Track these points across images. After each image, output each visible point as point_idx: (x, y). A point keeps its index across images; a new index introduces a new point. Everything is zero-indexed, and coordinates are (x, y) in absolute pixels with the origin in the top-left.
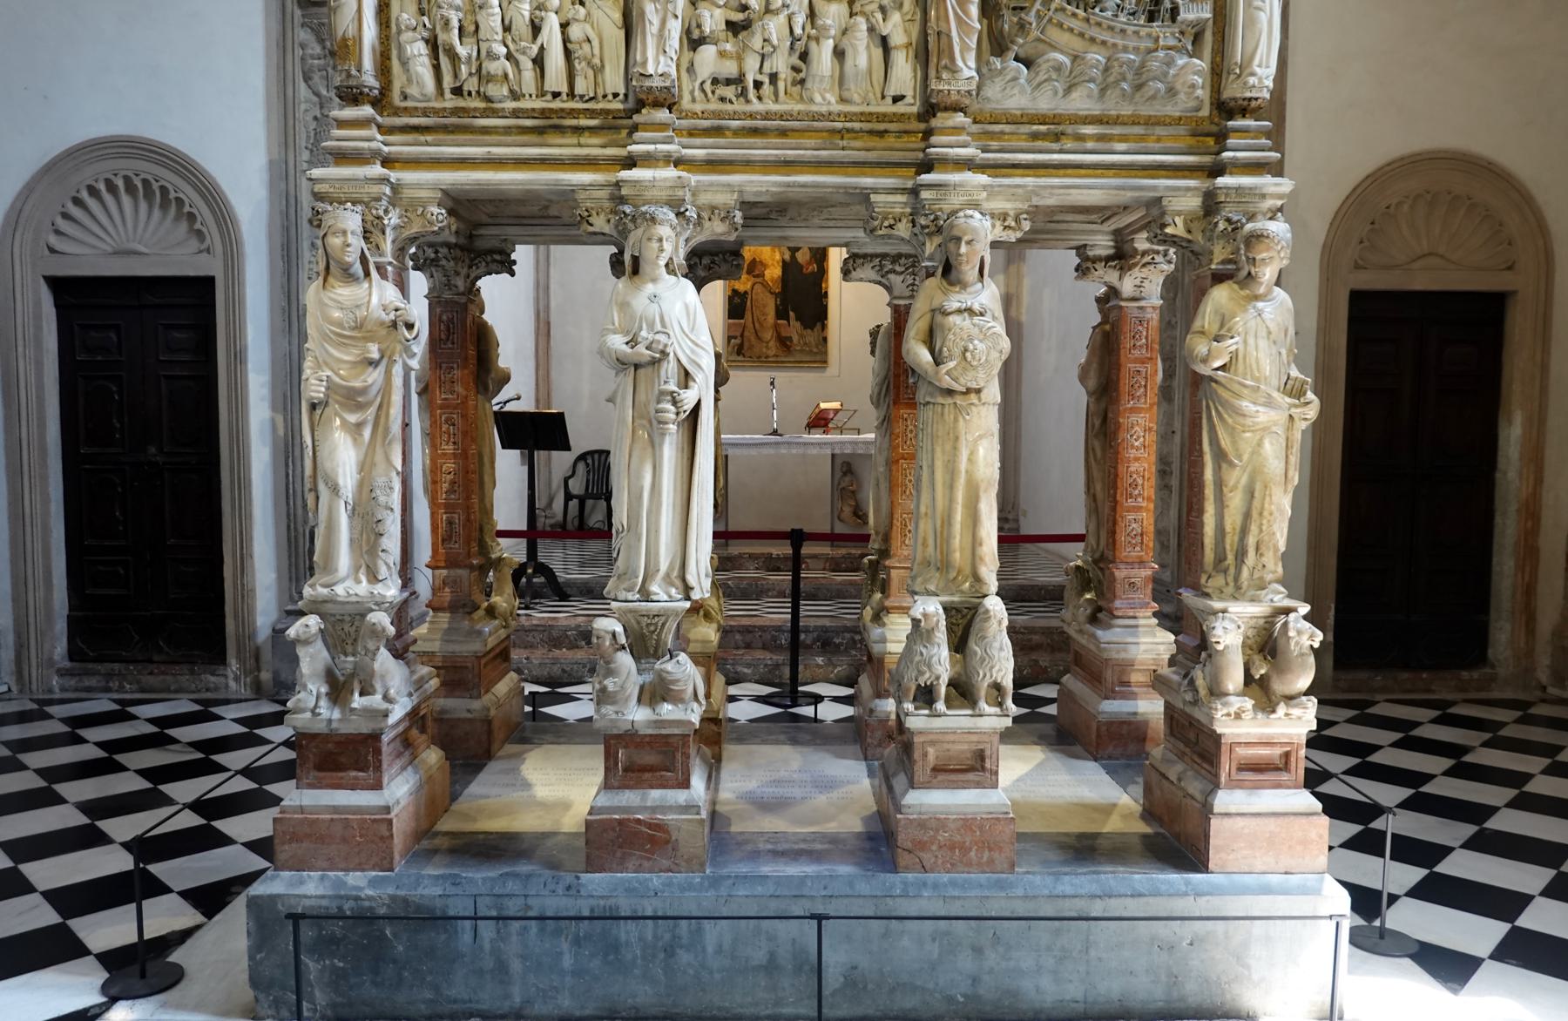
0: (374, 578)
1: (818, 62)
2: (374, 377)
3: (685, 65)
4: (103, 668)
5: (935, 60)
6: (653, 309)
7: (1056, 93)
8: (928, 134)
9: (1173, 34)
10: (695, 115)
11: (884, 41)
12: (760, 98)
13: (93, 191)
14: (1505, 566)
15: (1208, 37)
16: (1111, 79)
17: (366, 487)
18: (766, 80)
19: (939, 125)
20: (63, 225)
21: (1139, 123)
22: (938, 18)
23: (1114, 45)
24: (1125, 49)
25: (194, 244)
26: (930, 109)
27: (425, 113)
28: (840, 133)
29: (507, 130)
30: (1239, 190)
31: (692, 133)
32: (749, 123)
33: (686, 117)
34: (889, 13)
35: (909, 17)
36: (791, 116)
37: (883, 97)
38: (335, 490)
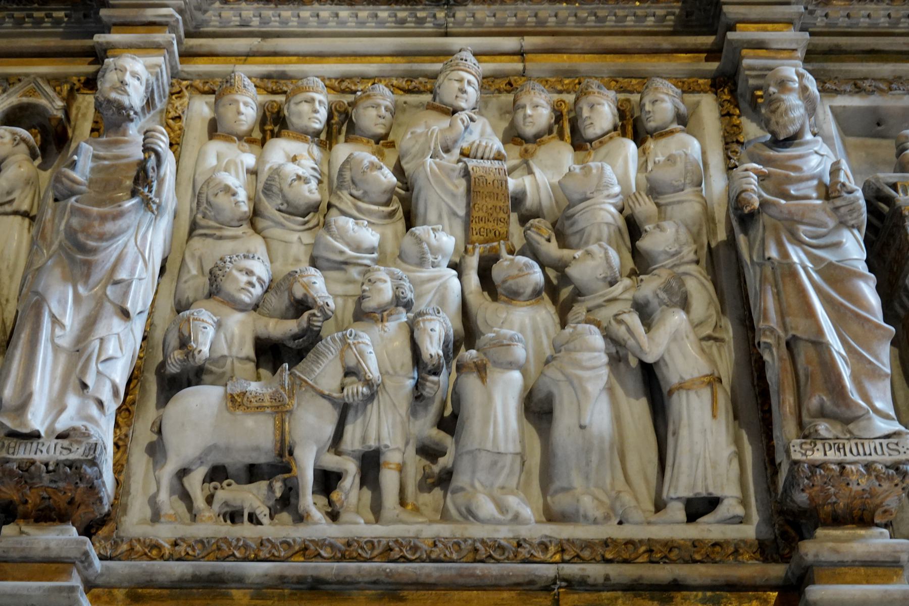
1: (486, 422)
3: (143, 434)
5: (789, 399)
10: (153, 549)
12: (334, 516)
18: (351, 467)
19: (826, 555)
22: (782, 314)
32: (296, 567)
33: (130, 555)
34: (657, 315)
35: (707, 331)
36: (415, 549)
37: (660, 506)
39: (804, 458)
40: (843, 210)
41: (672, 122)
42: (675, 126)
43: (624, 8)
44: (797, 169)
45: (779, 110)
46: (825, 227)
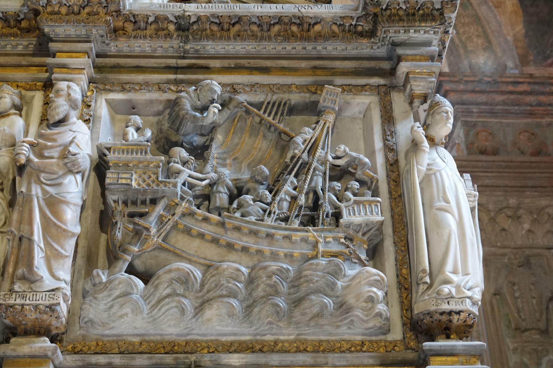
7: (183, 311)
9: (336, 239)
16: (260, 292)
21: (305, 350)
22: (20, 222)
23: (259, 252)
24: (274, 256)
39: (4, 302)
40: (69, 165)
41: (10, 109)
42: (13, 111)
43: (6, 41)
44: (54, 140)
45: (52, 108)
46: (57, 174)
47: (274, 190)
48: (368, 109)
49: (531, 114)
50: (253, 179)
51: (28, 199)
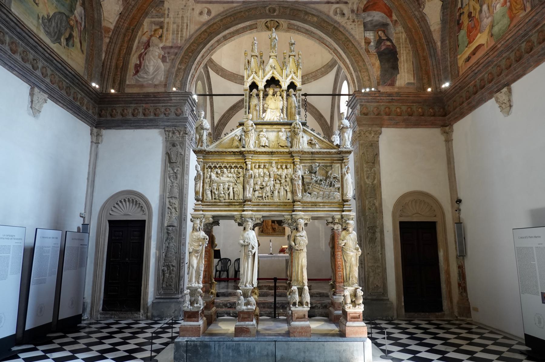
0: (199, 283)
2: (201, 248)
4: (110, 312)
6: (248, 236)
8: (294, 205)
10: (255, 202)
11: (286, 190)
13: (121, 202)
14: (443, 286)
15: (340, 189)
17: (198, 267)
20: (113, 208)
25: (142, 213)
26: (294, 201)
27: (209, 202)
28: (279, 205)
29: (223, 205)
30: (346, 215)
31: (254, 205)
32: (264, 204)
38: (193, 267)
47: (326, 180)
48: (338, 167)
49: (378, 102)
50: (323, 179)
51: (295, 184)
